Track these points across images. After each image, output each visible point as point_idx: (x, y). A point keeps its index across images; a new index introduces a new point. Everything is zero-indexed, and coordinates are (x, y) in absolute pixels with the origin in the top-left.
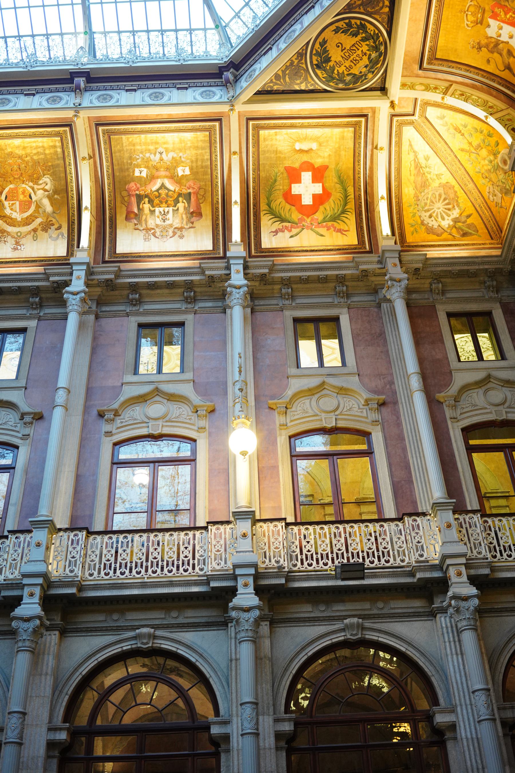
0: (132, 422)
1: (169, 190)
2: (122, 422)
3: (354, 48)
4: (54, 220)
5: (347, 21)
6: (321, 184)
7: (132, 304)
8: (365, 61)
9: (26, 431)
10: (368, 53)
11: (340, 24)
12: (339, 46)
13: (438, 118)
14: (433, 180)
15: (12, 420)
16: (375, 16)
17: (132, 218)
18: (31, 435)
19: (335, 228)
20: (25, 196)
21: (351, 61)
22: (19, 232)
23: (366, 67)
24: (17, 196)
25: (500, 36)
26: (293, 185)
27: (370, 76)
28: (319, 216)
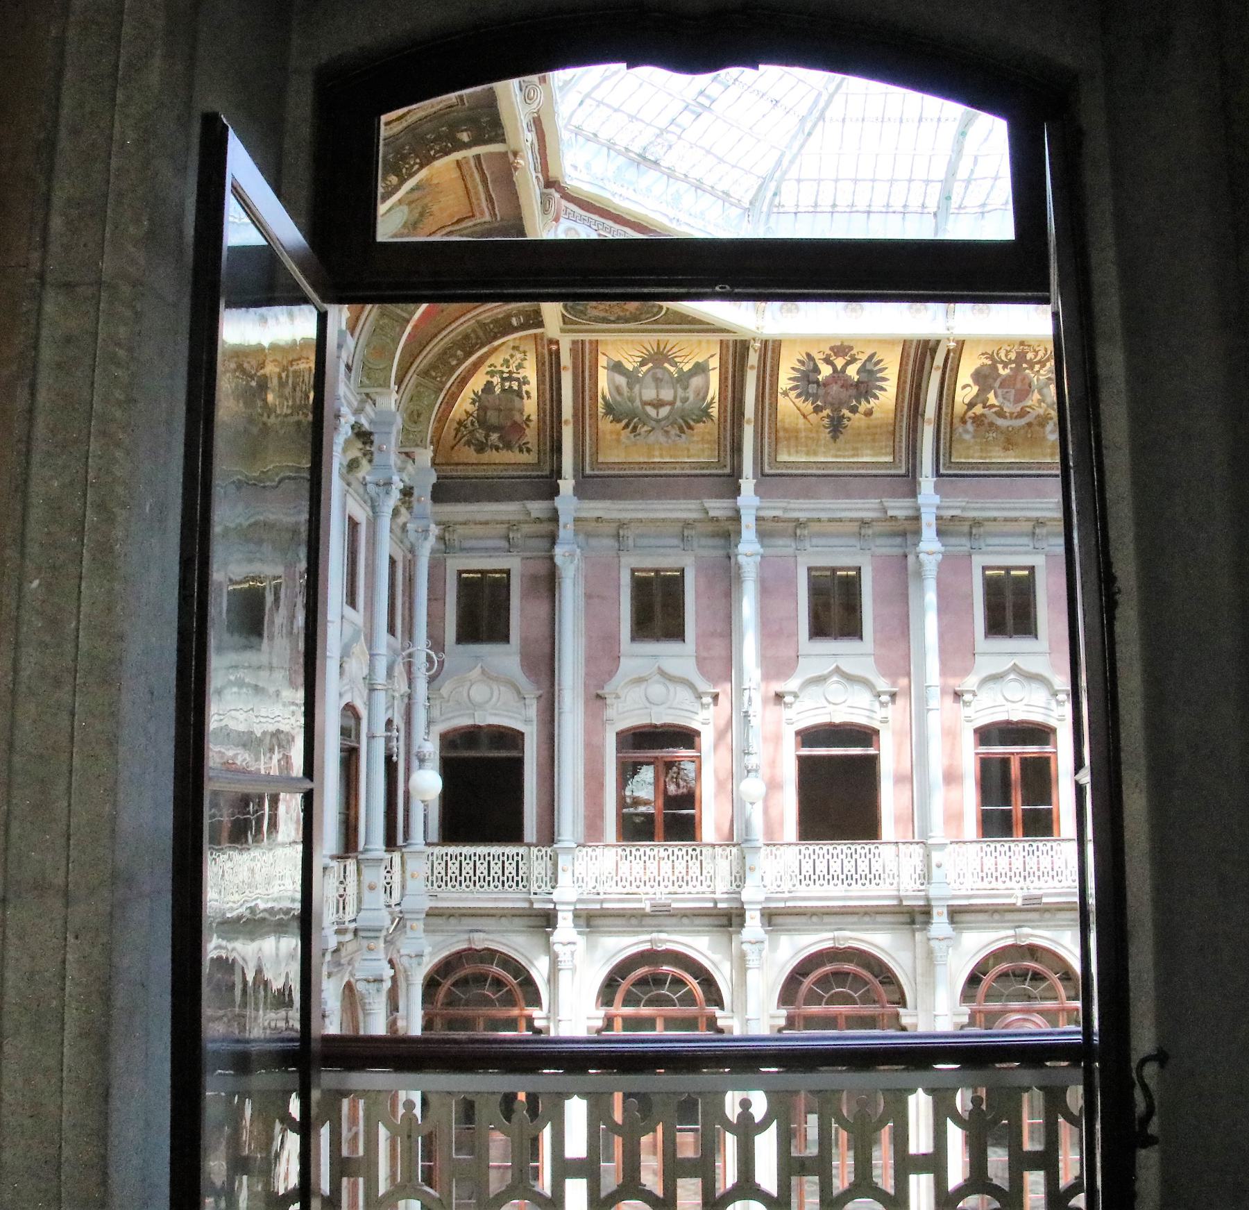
24: (1014, 384)
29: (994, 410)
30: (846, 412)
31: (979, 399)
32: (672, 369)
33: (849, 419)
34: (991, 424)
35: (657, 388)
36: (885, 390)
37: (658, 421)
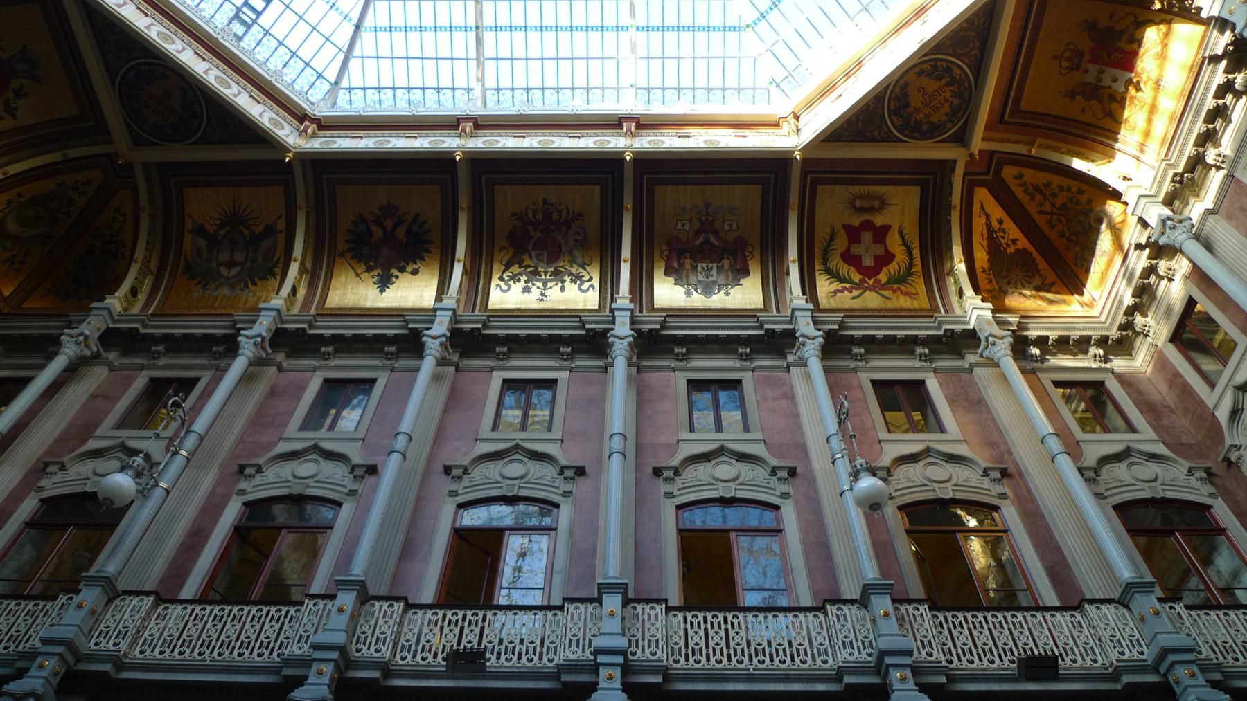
0: (697, 483)
1: (714, 245)
2: (684, 483)
3: (937, 94)
5: (932, 63)
6: (883, 245)
7: (677, 359)
8: (947, 108)
9: (568, 487)
10: (950, 99)
11: (925, 66)
12: (920, 91)
13: (1016, 177)
14: (1008, 245)
15: (550, 474)
16: (963, 59)
18: (574, 492)
19: (902, 291)
21: (932, 108)
23: (946, 115)
25: (1100, 80)
26: (851, 245)
27: (949, 125)
28: (883, 277)
32: (246, 232)
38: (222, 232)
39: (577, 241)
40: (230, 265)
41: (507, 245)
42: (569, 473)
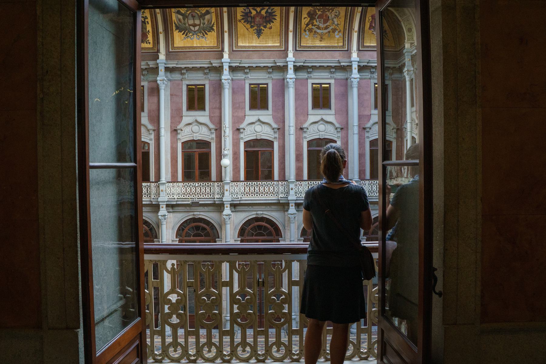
4: (338, 28)
17: (372, 28)
20: (326, 17)
22: (322, 32)
29: (316, 26)
30: (262, 27)
31: (311, 22)
32: (198, 13)
33: (264, 30)
34: (315, 32)
35: (194, 20)
36: (276, 19)
37: (195, 32)
38: (188, 12)
39: (335, 15)
40: (195, 25)
41: (307, 17)
42: (339, 130)
